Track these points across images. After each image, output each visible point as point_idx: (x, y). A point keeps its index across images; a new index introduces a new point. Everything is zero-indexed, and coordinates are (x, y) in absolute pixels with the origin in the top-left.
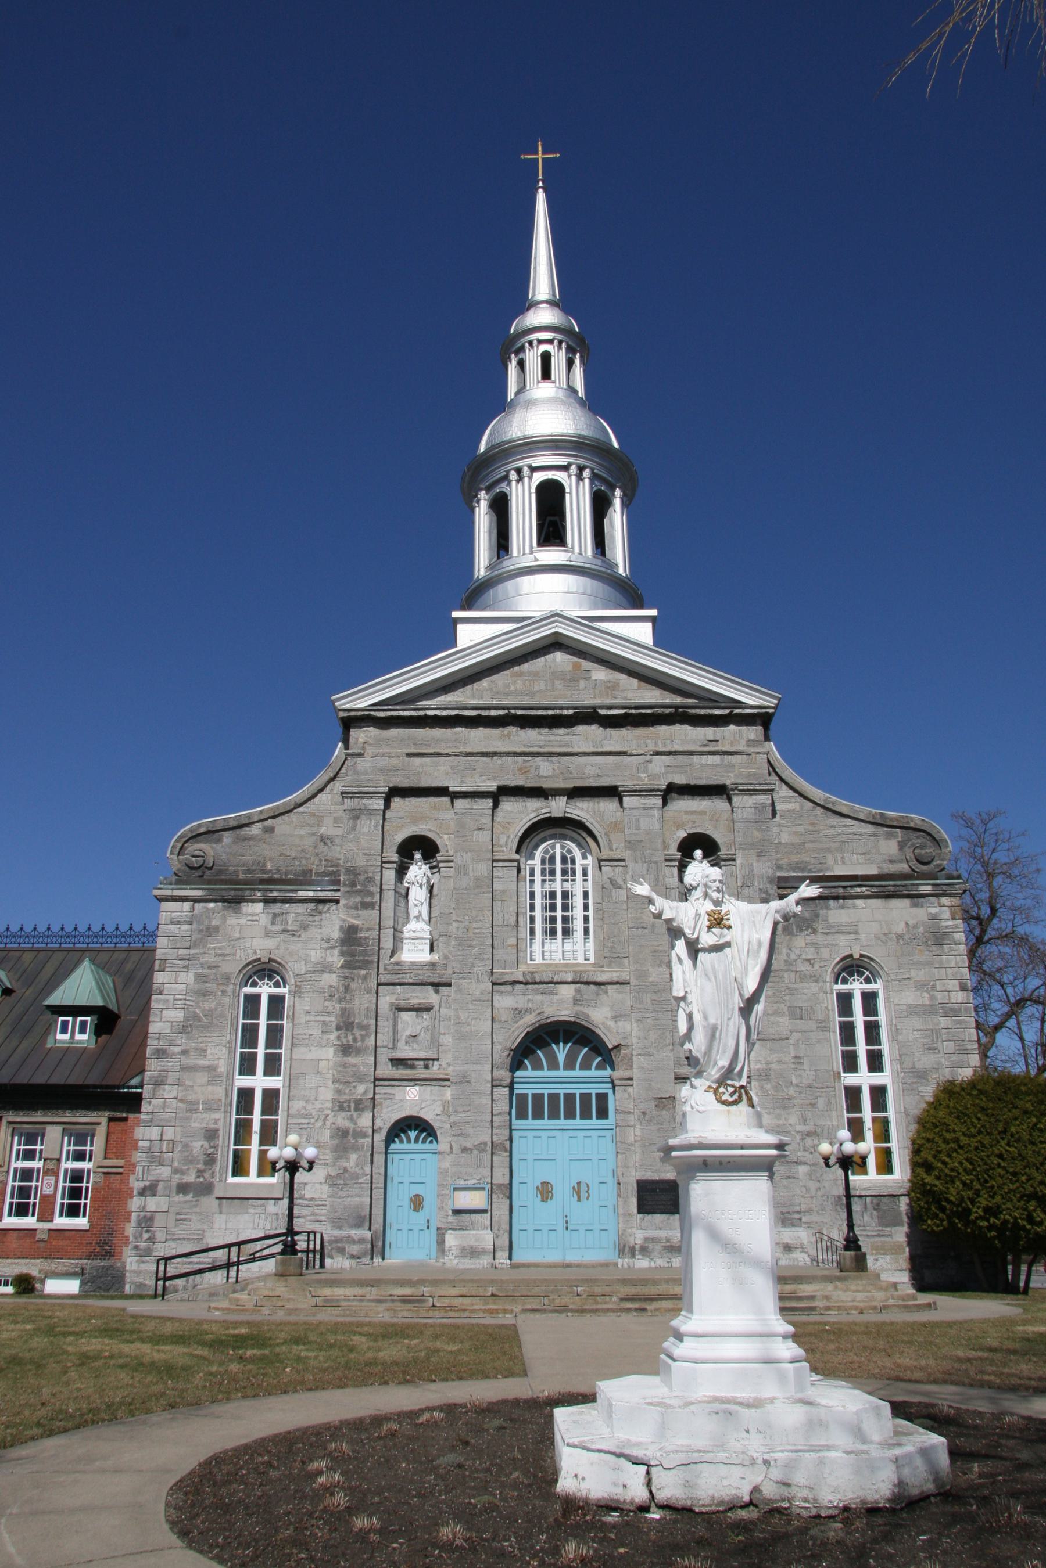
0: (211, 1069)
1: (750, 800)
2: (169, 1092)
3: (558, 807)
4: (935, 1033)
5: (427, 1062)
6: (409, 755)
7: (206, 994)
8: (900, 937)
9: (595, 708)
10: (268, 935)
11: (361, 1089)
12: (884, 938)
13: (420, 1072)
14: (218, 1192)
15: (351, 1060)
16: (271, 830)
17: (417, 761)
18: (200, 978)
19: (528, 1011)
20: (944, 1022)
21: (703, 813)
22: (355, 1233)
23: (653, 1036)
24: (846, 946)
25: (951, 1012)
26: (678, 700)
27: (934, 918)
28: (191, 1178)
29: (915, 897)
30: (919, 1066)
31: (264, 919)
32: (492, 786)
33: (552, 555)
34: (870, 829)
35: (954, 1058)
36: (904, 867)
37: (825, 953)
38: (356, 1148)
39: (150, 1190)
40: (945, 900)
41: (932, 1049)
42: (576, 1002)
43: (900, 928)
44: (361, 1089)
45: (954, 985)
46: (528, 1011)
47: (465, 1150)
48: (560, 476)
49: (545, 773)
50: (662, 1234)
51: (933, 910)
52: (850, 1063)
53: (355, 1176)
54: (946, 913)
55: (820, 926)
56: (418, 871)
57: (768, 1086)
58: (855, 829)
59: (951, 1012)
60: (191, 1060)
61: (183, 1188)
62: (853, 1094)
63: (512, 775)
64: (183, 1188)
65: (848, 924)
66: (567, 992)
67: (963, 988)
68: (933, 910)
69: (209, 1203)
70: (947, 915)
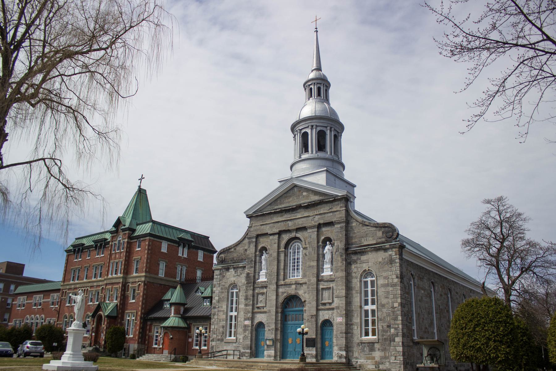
0: (223, 311)
1: (339, 226)
2: (216, 317)
3: (293, 235)
4: (388, 292)
5: (330, 304)
6: (261, 225)
7: (223, 292)
8: (380, 262)
9: (300, 204)
10: (234, 277)
11: (249, 315)
12: (376, 263)
13: (262, 310)
14: (225, 341)
15: (247, 308)
16: (235, 249)
17: (263, 227)
18: (222, 289)
19: (285, 292)
20: (391, 289)
21: (328, 231)
22: (247, 351)
23: (311, 298)
24: (365, 267)
25: (393, 285)
26: (321, 198)
27: (390, 255)
28: (220, 337)
29: (386, 250)
30: (383, 303)
31: (233, 272)
32: (276, 231)
33: (321, 154)
34: (374, 229)
35: (393, 300)
36: (383, 240)
37: (359, 269)
38: (248, 330)
39: (213, 340)
40: (394, 250)
41: (387, 297)
42: (296, 289)
43: (380, 260)
44: (249, 315)
45: (394, 276)
46: (285, 292)
47: (269, 330)
48: (324, 129)
49: (291, 225)
50: (310, 352)
51: (390, 253)
52: (366, 303)
53: (247, 337)
54: (394, 253)
55: (358, 261)
56: (328, 247)
57: (339, 311)
58: (370, 229)
59: (393, 285)
60: (220, 309)
61: (218, 340)
62: (366, 312)
63: (282, 227)
64: (218, 340)
65: (366, 260)
66: (294, 286)
67: (397, 277)
68: (390, 253)
69: (223, 343)
70: (394, 254)
